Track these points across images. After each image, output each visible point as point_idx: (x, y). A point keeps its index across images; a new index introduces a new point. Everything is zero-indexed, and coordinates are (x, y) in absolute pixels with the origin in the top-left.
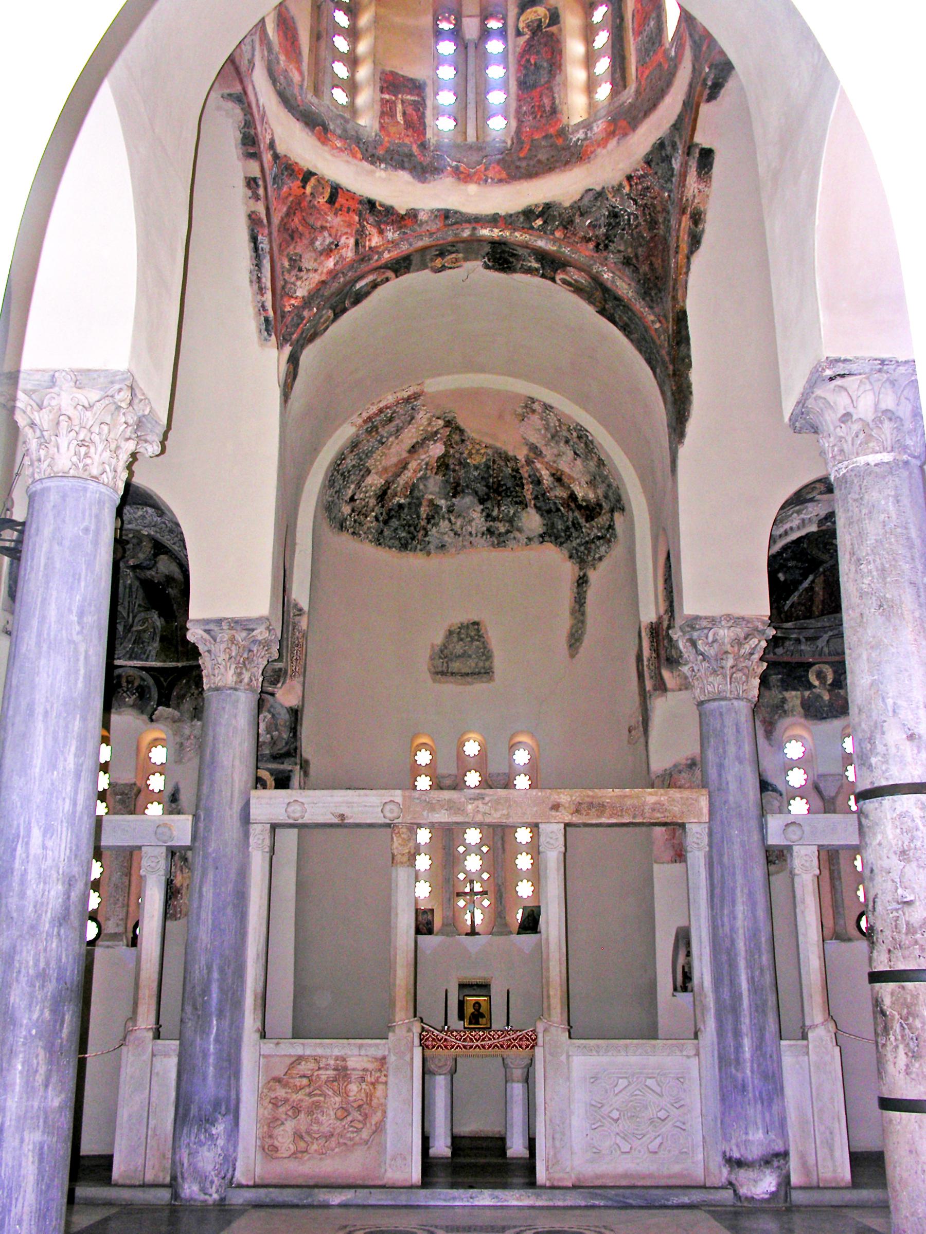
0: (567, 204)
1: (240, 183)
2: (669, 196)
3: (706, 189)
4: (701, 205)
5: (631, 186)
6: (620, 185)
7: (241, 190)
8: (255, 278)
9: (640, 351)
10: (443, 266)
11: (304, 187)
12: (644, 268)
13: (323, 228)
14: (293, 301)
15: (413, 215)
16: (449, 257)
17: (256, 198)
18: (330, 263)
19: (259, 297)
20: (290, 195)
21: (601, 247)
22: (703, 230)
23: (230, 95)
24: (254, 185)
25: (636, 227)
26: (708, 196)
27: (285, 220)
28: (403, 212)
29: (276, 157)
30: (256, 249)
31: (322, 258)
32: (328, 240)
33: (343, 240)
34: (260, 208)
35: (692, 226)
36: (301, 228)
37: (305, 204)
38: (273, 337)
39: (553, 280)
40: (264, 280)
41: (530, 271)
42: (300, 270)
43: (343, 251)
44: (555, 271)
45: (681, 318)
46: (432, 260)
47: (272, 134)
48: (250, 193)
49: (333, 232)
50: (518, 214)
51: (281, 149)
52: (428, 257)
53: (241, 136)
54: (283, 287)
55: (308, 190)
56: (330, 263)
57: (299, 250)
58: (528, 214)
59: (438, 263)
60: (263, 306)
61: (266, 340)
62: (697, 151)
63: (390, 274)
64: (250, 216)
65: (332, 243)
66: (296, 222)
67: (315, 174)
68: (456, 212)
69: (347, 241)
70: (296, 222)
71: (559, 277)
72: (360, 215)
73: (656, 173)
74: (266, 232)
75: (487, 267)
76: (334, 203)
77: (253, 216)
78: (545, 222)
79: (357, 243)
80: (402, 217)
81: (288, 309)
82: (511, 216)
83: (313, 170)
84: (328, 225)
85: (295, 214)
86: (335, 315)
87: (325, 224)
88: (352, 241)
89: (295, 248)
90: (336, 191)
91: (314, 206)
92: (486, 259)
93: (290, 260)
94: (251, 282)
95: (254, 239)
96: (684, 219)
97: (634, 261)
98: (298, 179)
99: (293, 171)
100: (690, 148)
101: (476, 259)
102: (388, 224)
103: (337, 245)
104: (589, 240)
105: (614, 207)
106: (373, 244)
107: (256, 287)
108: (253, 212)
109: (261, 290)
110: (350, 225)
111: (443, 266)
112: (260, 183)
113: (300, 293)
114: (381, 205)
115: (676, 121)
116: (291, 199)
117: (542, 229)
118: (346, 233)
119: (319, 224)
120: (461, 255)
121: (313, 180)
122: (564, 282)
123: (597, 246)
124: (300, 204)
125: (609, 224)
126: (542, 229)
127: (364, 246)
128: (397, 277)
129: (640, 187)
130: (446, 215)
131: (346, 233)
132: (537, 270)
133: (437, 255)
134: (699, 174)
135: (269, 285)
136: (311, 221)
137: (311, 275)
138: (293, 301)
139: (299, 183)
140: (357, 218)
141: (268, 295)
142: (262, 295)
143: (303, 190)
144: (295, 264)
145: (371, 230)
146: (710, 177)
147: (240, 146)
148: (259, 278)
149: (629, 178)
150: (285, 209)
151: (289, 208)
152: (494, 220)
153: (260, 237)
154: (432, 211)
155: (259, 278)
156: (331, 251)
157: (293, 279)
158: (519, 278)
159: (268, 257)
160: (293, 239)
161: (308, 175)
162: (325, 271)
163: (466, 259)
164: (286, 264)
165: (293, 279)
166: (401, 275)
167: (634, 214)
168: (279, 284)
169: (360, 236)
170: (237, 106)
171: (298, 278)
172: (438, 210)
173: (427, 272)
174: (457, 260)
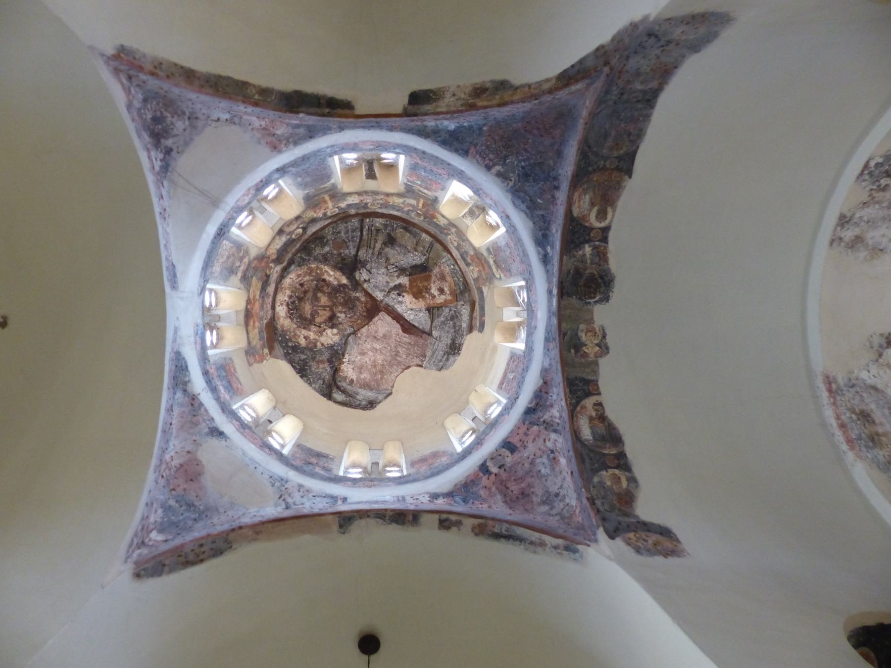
0: (531, 224)
1: (444, 535)
2: (484, 125)
3: (451, 90)
4: (467, 91)
5: (494, 165)
6: (499, 175)
7: (451, 536)
8: (532, 548)
9: (647, 117)
10: (597, 345)
11: (491, 473)
12: (557, 132)
13: (532, 463)
14: (577, 511)
15: (545, 372)
16: (583, 337)
17: (458, 524)
18: (563, 461)
19: (547, 549)
20: (490, 489)
21: (556, 183)
22: (492, 82)
23: (341, 526)
24: (447, 524)
25: (526, 150)
26: (459, 86)
27: (508, 499)
28: (541, 382)
29: (450, 495)
30: (508, 537)
31: (557, 469)
32: (545, 460)
33: (549, 444)
34: (469, 523)
35: (488, 93)
36: (523, 485)
37: (504, 476)
38: (580, 547)
39: (606, 229)
40: (533, 539)
41: (601, 255)
42: (557, 495)
43: (559, 445)
44: (592, 229)
45: (567, 78)
46: (585, 355)
47: (427, 493)
48: (454, 529)
49: (539, 453)
50: (547, 271)
51: (446, 489)
52: (577, 360)
53: (394, 525)
54: (563, 518)
55: (494, 470)
56: (563, 461)
57: (540, 492)
58: (545, 260)
59: (591, 350)
60: (556, 547)
61: (581, 557)
62: (410, 107)
63: (589, 402)
64: (476, 535)
65: (548, 456)
66: (515, 488)
67: (485, 461)
68: (546, 330)
69: (552, 441)
70: (515, 488)
71: (593, 221)
72: (532, 424)
73: (471, 143)
74: (491, 523)
75: (607, 299)
76: (515, 447)
77: (477, 531)
78: (548, 244)
79: (555, 431)
80: (545, 383)
81: (580, 519)
82: (548, 278)
83: (481, 462)
84: (532, 457)
85: (507, 488)
86: (617, 467)
87: (530, 460)
88: (553, 436)
89: (537, 496)
90: (508, 445)
91: (510, 468)
92: (592, 301)
93: (544, 503)
94: (535, 552)
95: (497, 536)
96: (480, 104)
97: (556, 147)
98: (481, 478)
99: (473, 481)
100: (406, 114)
101: (591, 312)
102: (547, 398)
103: (552, 452)
104: (553, 197)
105: (519, 175)
106: (557, 414)
107: (539, 549)
108: (473, 531)
109: (542, 544)
110: (538, 436)
111: (597, 345)
112: (444, 516)
113: (574, 503)
114: (531, 402)
115: (413, 134)
116: (494, 489)
117: (553, 248)
118: (545, 441)
119: (527, 465)
120: (582, 326)
121: (489, 464)
122: (602, 215)
123: (557, 188)
124: (502, 482)
125: (535, 180)
126: (553, 248)
127: (558, 424)
128: (599, 394)
129: (491, 156)
130: (547, 340)
131: (545, 441)
132: (595, 248)
133: (577, 351)
134: (436, 100)
135: (537, 535)
136: (520, 473)
137: (565, 485)
138: (577, 511)
139: (485, 478)
140: (535, 427)
141: (548, 539)
142: (546, 545)
143: (493, 476)
144: (549, 499)
145: (546, 417)
146: (439, 89)
147: (405, 527)
148: (532, 543)
149: (488, 168)
150: (499, 497)
151: (500, 492)
152: (550, 292)
153: (496, 530)
154: (545, 354)
155: (532, 543)
156: (554, 458)
157: (561, 505)
158: (614, 264)
159: (514, 527)
160: (528, 495)
161: (484, 468)
162: (566, 468)
163: (591, 321)
164: (545, 508)
165: (561, 505)
166: (598, 388)
167: (517, 157)
168: (553, 522)
169: (549, 426)
170: (356, 523)
171: (563, 500)
172: (545, 347)
173: (602, 362)
174: (591, 331)
